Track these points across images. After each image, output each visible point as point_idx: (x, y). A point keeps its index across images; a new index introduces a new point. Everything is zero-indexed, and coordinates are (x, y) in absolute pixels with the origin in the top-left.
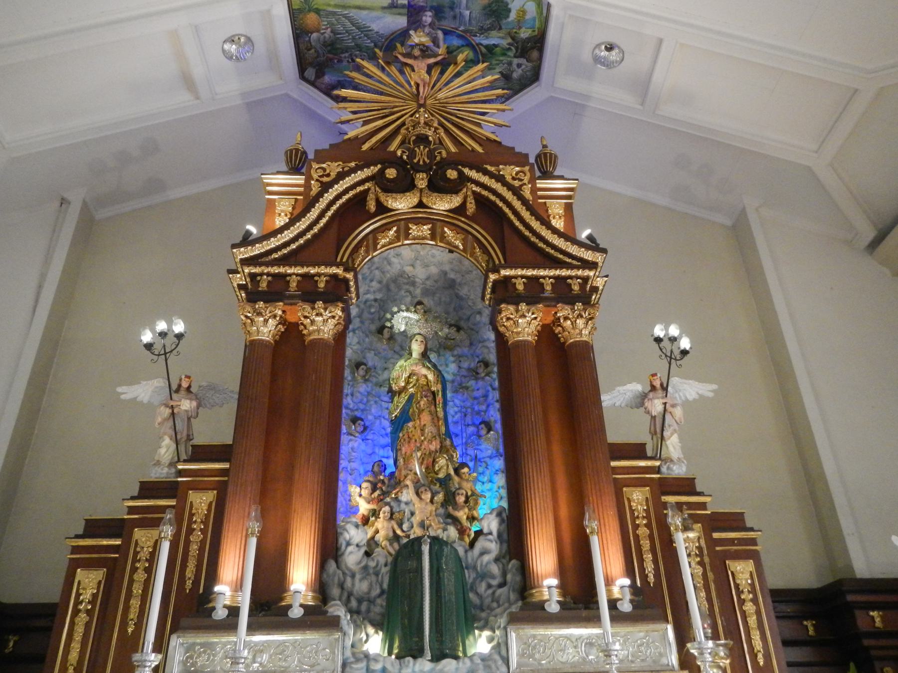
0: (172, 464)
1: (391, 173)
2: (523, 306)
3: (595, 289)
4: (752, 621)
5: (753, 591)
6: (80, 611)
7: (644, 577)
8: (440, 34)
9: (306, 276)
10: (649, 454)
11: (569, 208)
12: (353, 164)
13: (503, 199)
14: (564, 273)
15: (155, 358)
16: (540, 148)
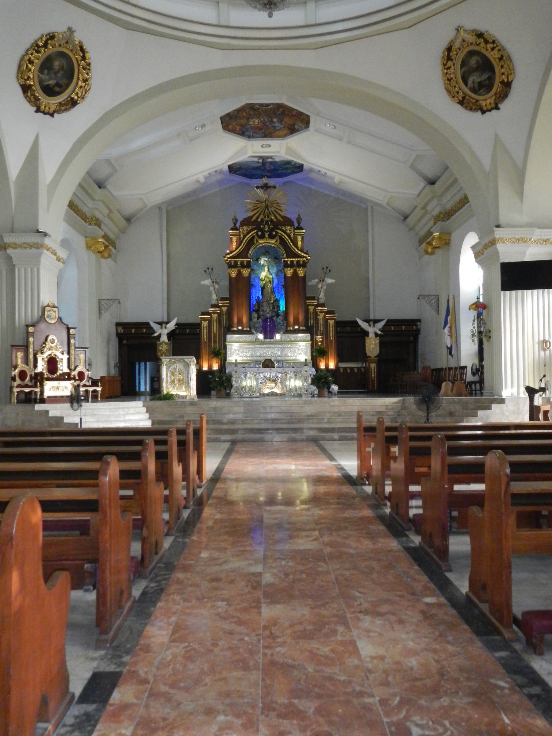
0: (216, 300)
1: (260, 233)
2: (289, 269)
3: (307, 259)
4: (331, 331)
5: (333, 326)
7: (310, 324)
8: (272, 166)
9: (242, 261)
10: (316, 298)
11: (302, 238)
12: (250, 228)
13: (286, 238)
14: (299, 259)
16: (298, 216)
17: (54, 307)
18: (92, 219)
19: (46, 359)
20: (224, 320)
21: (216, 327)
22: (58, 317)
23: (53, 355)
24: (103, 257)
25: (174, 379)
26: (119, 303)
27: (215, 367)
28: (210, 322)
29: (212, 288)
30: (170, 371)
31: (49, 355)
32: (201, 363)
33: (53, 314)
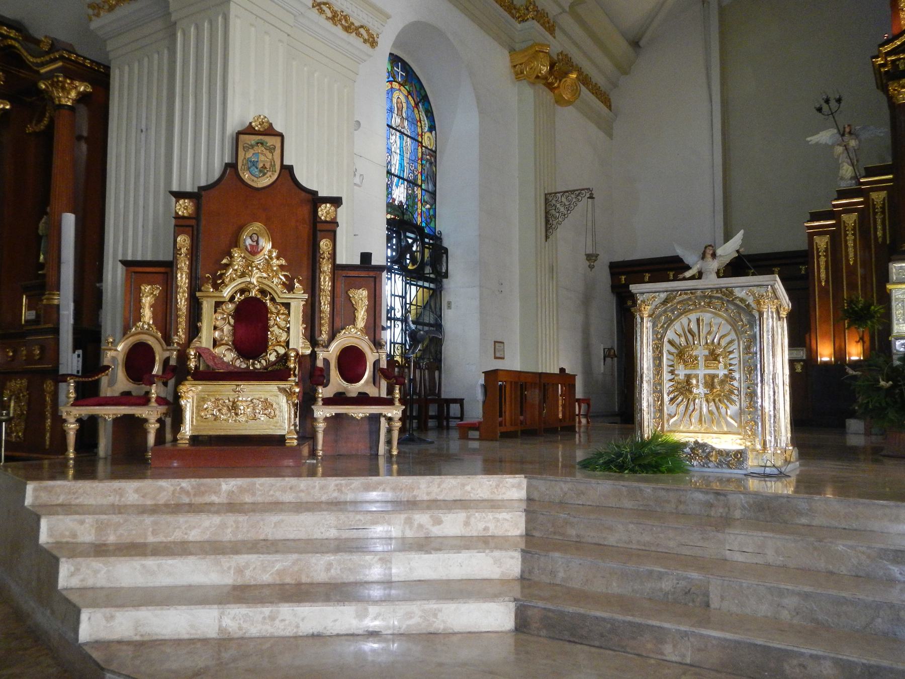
0: (852, 178)
6: (820, 256)
15: (827, 117)
17: (270, 131)
18: (527, 9)
19: (231, 306)
20: (879, 227)
21: (855, 247)
22: (283, 167)
23: (254, 293)
24: (560, 101)
25: (688, 377)
26: (591, 197)
27: (855, 352)
28: (836, 238)
29: (840, 149)
30: (671, 342)
31: (242, 291)
32: (813, 342)
33: (264, 158)
